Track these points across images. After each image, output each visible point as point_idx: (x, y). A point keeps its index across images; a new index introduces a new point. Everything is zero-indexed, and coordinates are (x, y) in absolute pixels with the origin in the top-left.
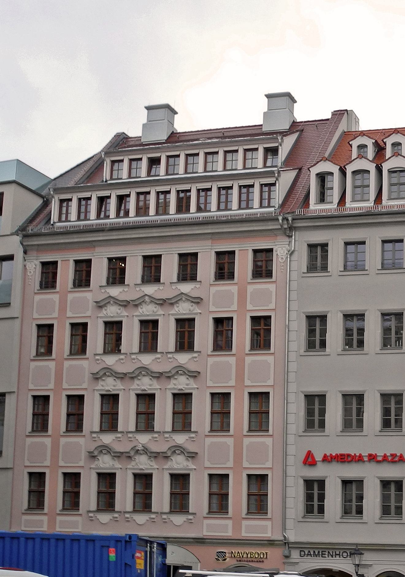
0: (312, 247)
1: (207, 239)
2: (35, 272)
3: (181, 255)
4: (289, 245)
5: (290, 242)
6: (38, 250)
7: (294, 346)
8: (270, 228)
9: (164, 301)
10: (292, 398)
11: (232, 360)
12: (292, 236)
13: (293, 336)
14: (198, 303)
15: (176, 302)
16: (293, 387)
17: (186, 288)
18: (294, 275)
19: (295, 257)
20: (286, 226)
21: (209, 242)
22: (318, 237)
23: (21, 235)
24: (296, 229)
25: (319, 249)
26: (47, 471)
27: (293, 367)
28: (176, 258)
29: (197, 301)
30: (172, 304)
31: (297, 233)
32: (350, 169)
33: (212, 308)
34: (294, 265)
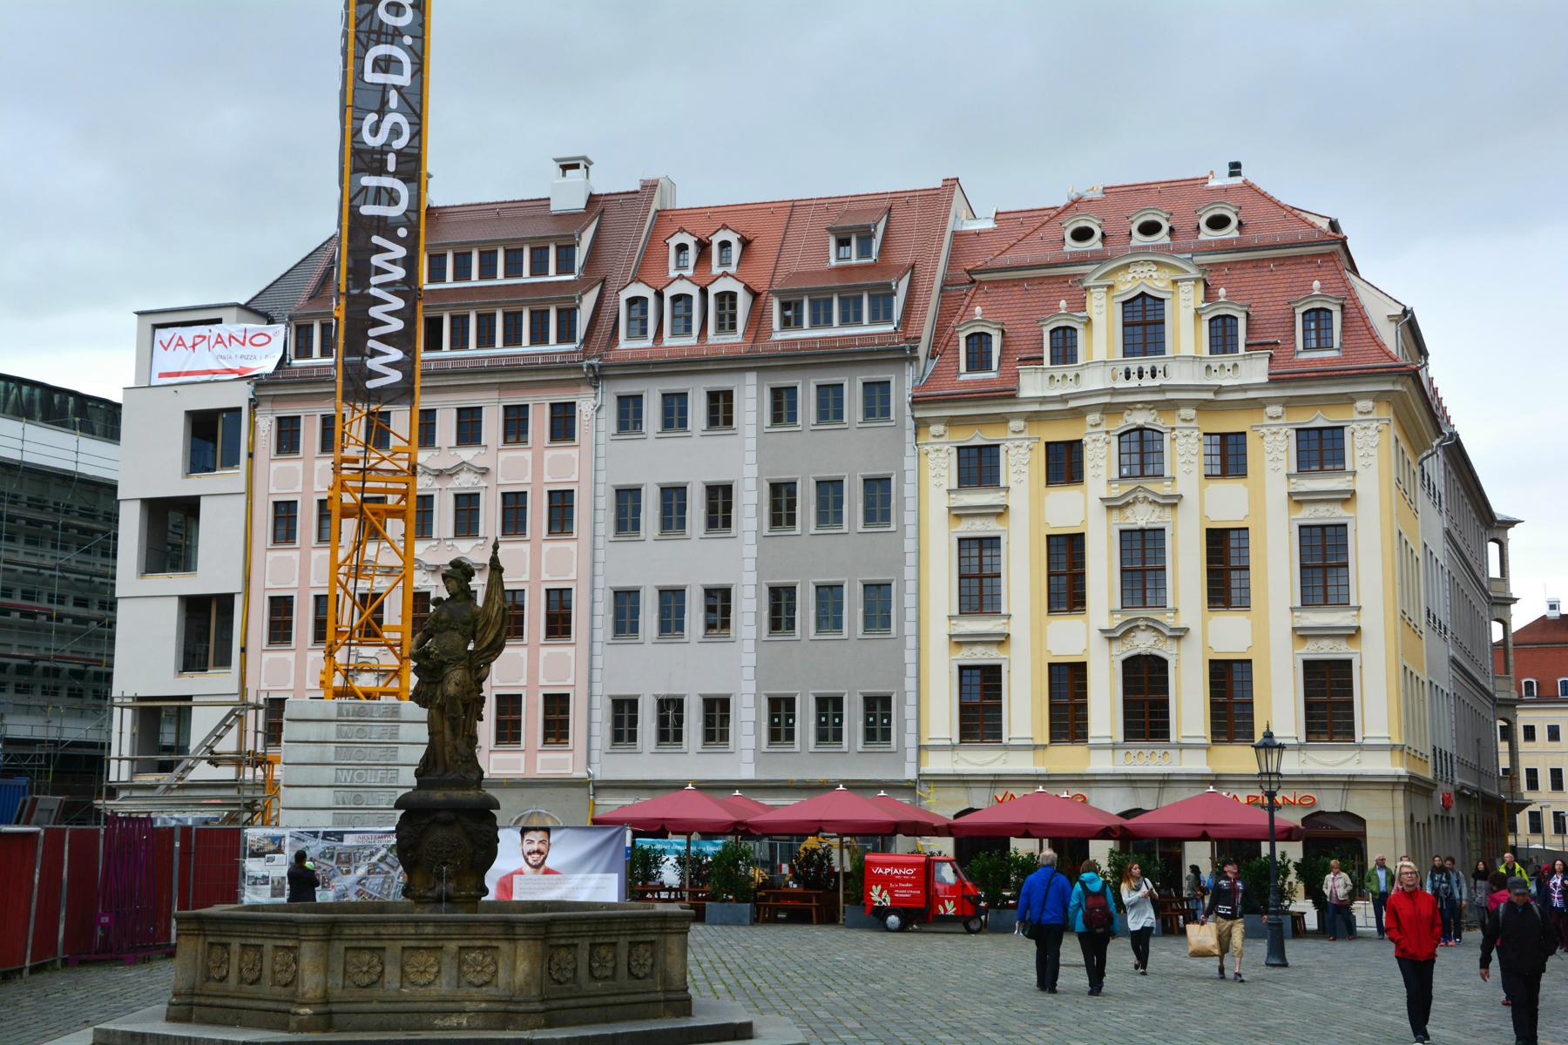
0: (622, 399)
1: (493, 389)
2: (270, 431)
3: (459, 410)
4: (595, 398)
5: (596, 394)
6: (272, 401)
7: (601, 529)
8: (572, 377)
9: (441, 471)
10: (599, 595)
11: (526, 547)
12: (598, 387)
13: (600, 516)
14: (483, 474)
15: (456, 473)
16: (600, 582)
17: (467, 454)
18: (602, 438)
19: (602, 414)
20: (591, 375)
21: (494, 395)
22: (629, 388)
23: (253, 384)
24: (604, 377)
25: (631, 403)
26: (290, 696)
27: (600, 555)
28: (454, 413)
29: (484, 472)
30: (451, 475)
31: (605, 383)
32: (668, 293)
33: (501, 481)
34: (602, 423)
